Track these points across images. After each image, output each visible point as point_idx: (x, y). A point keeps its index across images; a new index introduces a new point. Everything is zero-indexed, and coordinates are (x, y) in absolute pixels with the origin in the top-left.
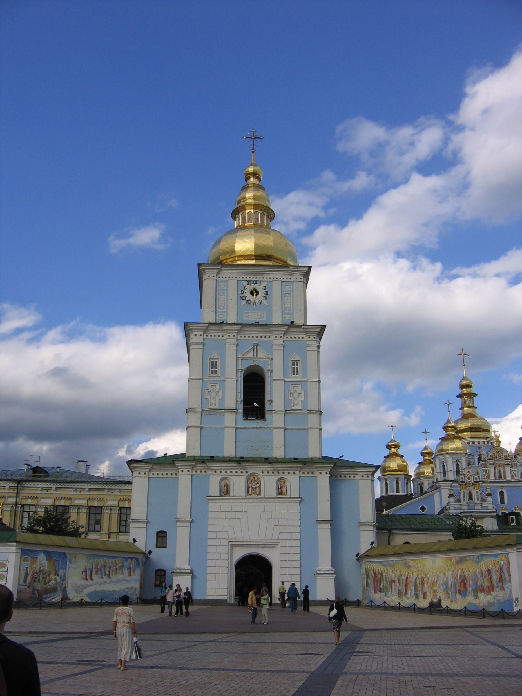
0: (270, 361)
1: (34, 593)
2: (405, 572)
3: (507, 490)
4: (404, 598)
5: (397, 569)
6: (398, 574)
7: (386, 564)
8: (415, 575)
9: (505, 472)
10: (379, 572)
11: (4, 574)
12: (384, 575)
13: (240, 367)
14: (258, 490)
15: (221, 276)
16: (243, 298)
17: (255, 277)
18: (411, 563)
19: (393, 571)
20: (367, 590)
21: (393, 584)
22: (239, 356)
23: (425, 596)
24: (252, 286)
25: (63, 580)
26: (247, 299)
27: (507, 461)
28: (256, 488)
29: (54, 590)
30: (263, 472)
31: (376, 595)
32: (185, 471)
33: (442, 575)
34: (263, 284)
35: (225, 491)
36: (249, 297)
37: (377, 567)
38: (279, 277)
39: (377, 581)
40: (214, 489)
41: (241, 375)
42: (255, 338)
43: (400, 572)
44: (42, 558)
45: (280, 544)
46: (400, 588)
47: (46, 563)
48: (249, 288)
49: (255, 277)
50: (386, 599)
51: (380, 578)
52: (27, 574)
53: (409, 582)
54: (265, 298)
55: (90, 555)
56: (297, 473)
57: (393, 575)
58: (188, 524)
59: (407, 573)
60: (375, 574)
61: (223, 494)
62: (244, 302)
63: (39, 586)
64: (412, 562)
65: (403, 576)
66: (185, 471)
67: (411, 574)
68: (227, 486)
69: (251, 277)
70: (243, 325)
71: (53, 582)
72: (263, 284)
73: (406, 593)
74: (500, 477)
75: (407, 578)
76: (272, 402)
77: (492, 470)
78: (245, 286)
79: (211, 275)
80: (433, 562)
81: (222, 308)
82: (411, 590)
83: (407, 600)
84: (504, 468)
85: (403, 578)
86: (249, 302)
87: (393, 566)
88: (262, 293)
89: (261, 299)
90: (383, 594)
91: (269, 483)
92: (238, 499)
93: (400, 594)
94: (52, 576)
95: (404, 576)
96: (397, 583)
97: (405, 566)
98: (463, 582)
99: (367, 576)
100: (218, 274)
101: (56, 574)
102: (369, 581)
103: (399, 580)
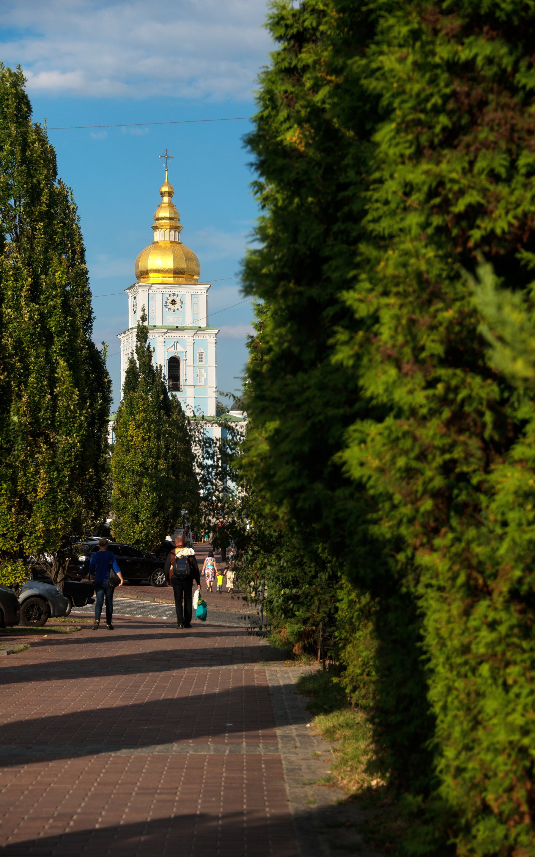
16: (167, 306)
34: (179, 297)
36: (170, 306)
48: (170, 299)
54: (181, 307)
62: (167, 309)
72: (179, 297)
86: (170, 310)
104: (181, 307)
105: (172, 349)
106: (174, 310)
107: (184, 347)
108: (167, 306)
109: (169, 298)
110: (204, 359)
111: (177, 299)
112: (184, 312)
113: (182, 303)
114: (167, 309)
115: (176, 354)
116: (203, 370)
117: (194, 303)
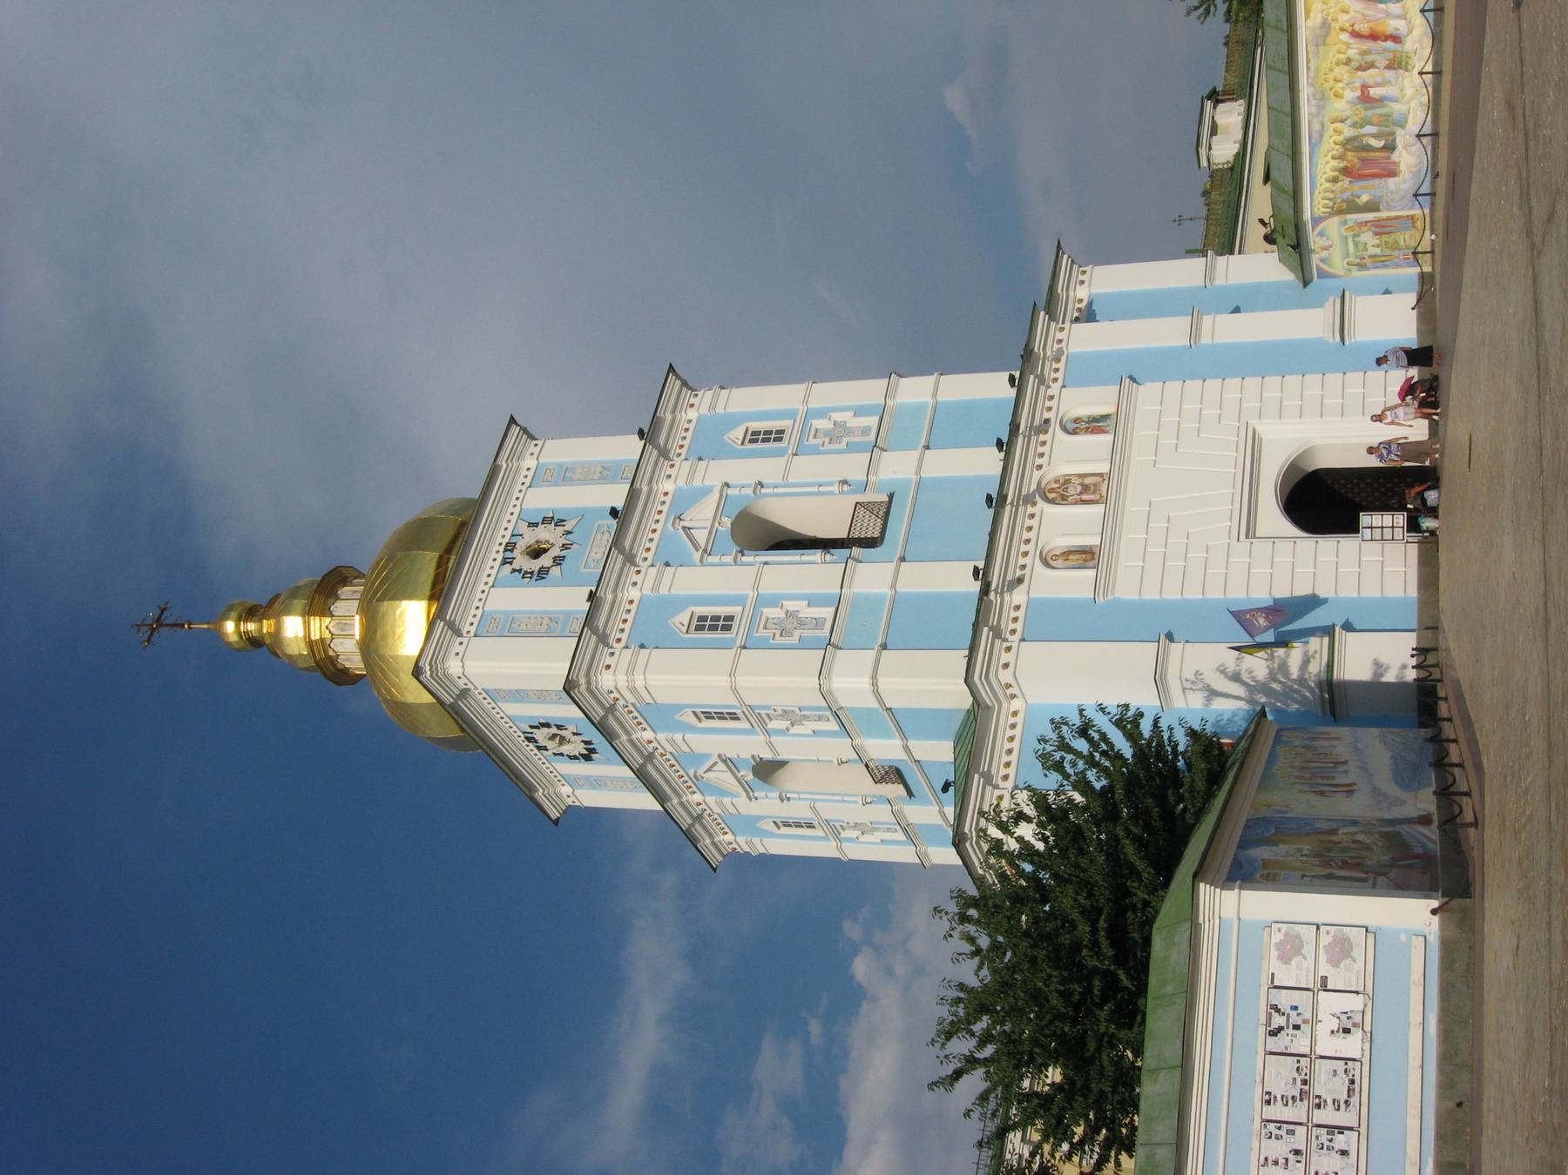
0: (730, 492)
1: (1411, 867)
4: (1409, 45)
5: (1331, 77)
6: (1341, 71)
7: (1317, 127)
10: (1341, 158)
11: (1325, 940)
12: (1348, 132)
13: (729, 559)
14: (1087, 481)
15: (467, 628)
16: (543, 573)
17: (497, 547)
18: (1316, 19)
19: (1336, 95)
20: (1389, 209)
21: (1375, 92)
22: (697, 556)
24: (516, 553)
25: (1355, 823)
28: (1082, 485)
30: (1040, 467)
31: (1402, 167)
35: (1086, 556)
36: (545, 560)
38: (516, 494)
39: (1366, 162)
40: (1075, 584)
42: (659, 527)
43: (1338, 64)
44: (1260, 853)
45: (1254, 422)
46: (1382, 61)
47: (1283, 848)
49: (497, 547)
50: (1413, 125)
51: (1357, 149)
52: (1330, 876)
53: (1363, 28)
54: (560, 522)
55: (1263, 778)
56: (1054, 389)
57: (1351, 95)
58: (1175, 648)
59: (1344, 37)
60: (1346, 171)
61: (1090, 564)
62: (555, 571)
63: (1379, 857)
64: (1312, 15)
65: (1352, 53)
67: (1344, 20)
68: (1067, 554)
69: (494, 555)
70: (617, 542)
71: (1360, 837)
73: (1396, 39)
75: (1356, 35)
76: (845, 482)
78: (514, 571)
79: (456, 648)
81: (553, 625)
82: (1388, 15)
83: (1417, 32)
85: (1355, 50)
86: (558, 561)
87: (1321, 98)
88: (545, 534)
89: (560, 530)
90: (1399, 142)
91: (1069, 457)
92: (1109, 526)
93: (1397, 64)
94: (1335, 838)
95: (1348, 46)
96: (1370, 76)
97: (1324, 44)
99: (1352, 207)
100: (458, 633)
101: (1334, 831)
102: (1365, 198)
103: (1361, 68)
104: (560, 522)
105: (701, 537)
106: (565, 547)
107: (706, 491)
108: (543, 573)
109: (516, 565)
110: (773, 425)
111: (530, 537)
112: (582, 514)
114: (555, 571)
115: (727, 522)
117: (564, 475)
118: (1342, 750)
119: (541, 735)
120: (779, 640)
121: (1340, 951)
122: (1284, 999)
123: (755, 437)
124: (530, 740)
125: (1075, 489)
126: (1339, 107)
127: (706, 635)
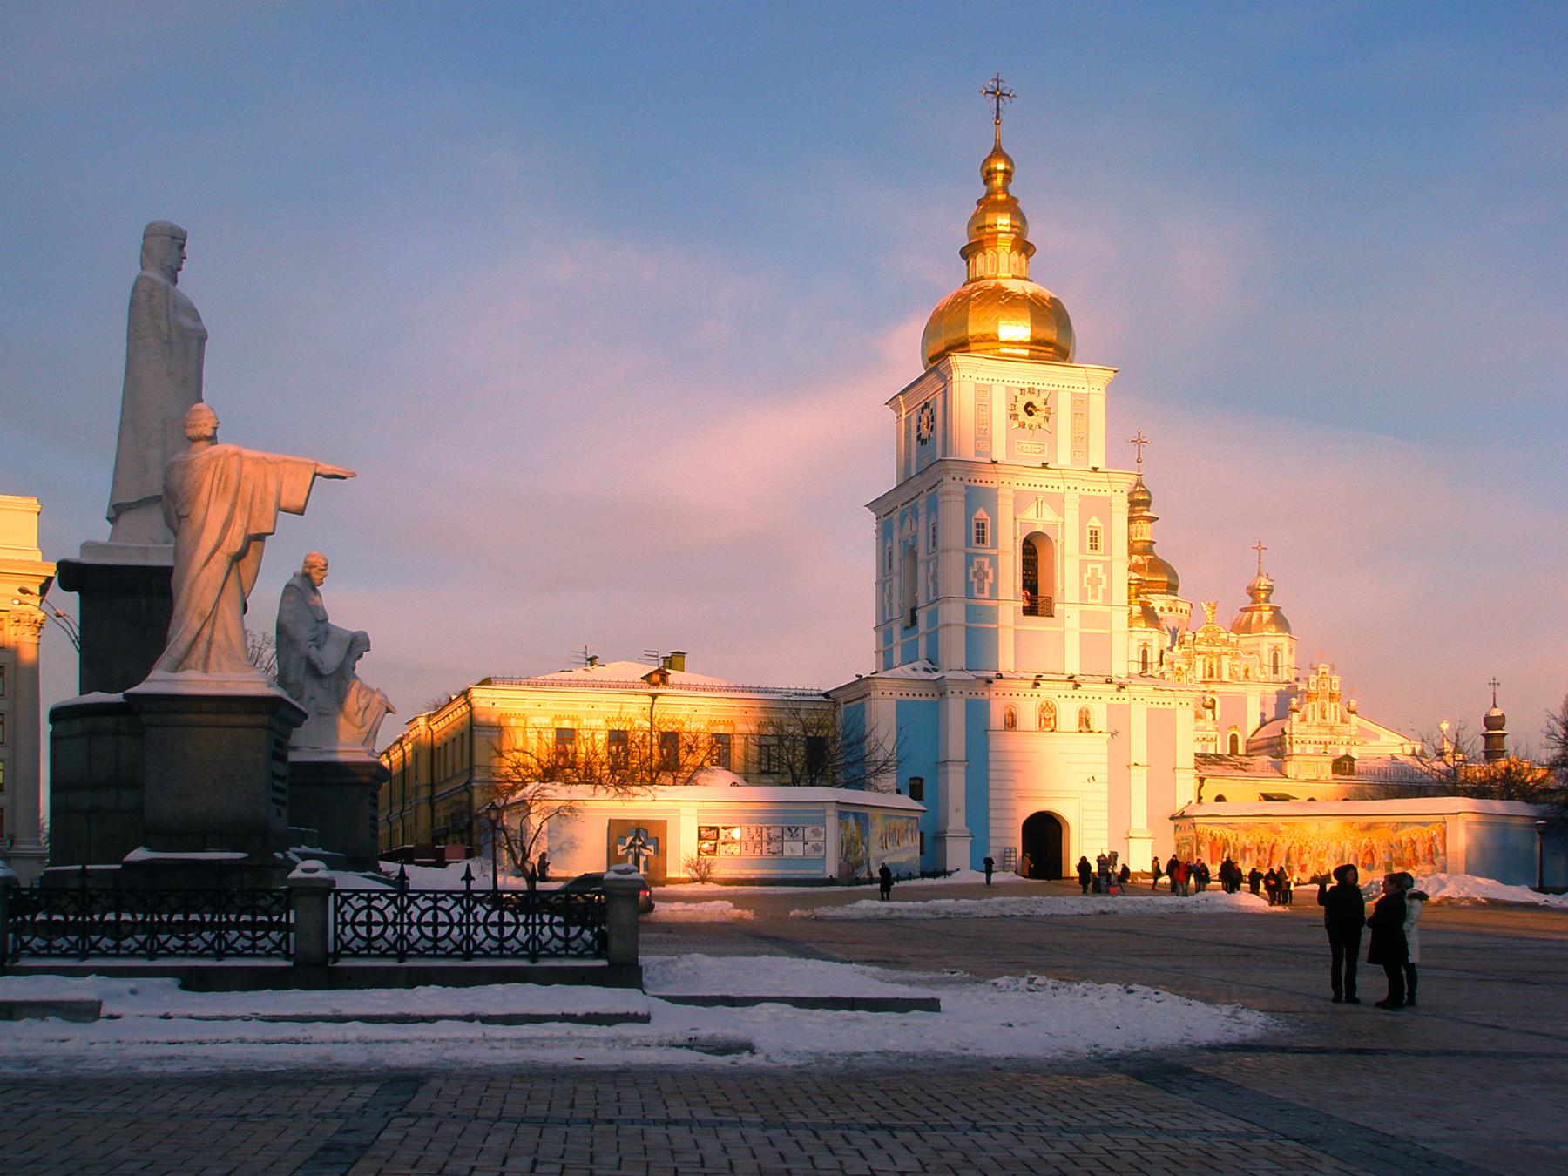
2: (1272, 838)
3: (1221, 699)
8: (1288, 843)
9: (1219, 668)
12: (1232, 842)
16: (1014, 416)
18: (1282, 828)
23: (1303, 868)
26: (1020, 419)
27: (1224, 649)
29: (859, 864)
32: (957, 692)
33: (1334, 845)
36: (1023, 416)
37: (1217, 831)
41: (1019, 546)
44: (852, 820)
63: (851, 859)
66: (957, 692)
67: (1280, 841)
68: (1012, 714)
74: (1211, 675)
77: (1199, 665)
80: (1321, 828)
84: (1219, 660)
86: (1023, 425)
89: (1041, 420)
98: (1371, 853)
108: (1014, 416)
110: (1101, 543)
111: (1038, 403)
112: (1053, 433)
113: (1048, 411)
114: (1016, 424)
115: (1039, 529)
116: (1100, 567)
118: (904, 844)
119: (927, 411)
120: (971, 570)
121: (816, 848)
122: (800, 832)
123: (1094, 533)
124: (927, 405)
125: (1047, 715)
126: (1243, 838)
127: (974, 529)
